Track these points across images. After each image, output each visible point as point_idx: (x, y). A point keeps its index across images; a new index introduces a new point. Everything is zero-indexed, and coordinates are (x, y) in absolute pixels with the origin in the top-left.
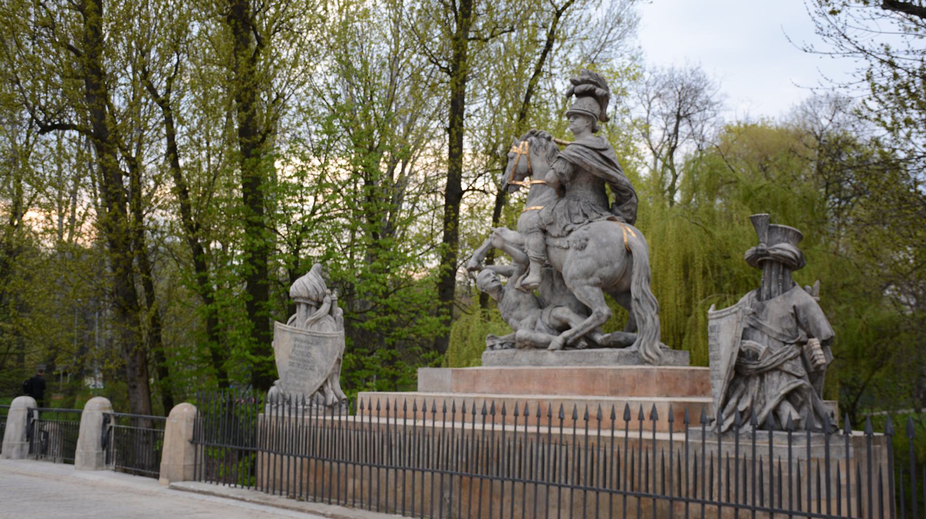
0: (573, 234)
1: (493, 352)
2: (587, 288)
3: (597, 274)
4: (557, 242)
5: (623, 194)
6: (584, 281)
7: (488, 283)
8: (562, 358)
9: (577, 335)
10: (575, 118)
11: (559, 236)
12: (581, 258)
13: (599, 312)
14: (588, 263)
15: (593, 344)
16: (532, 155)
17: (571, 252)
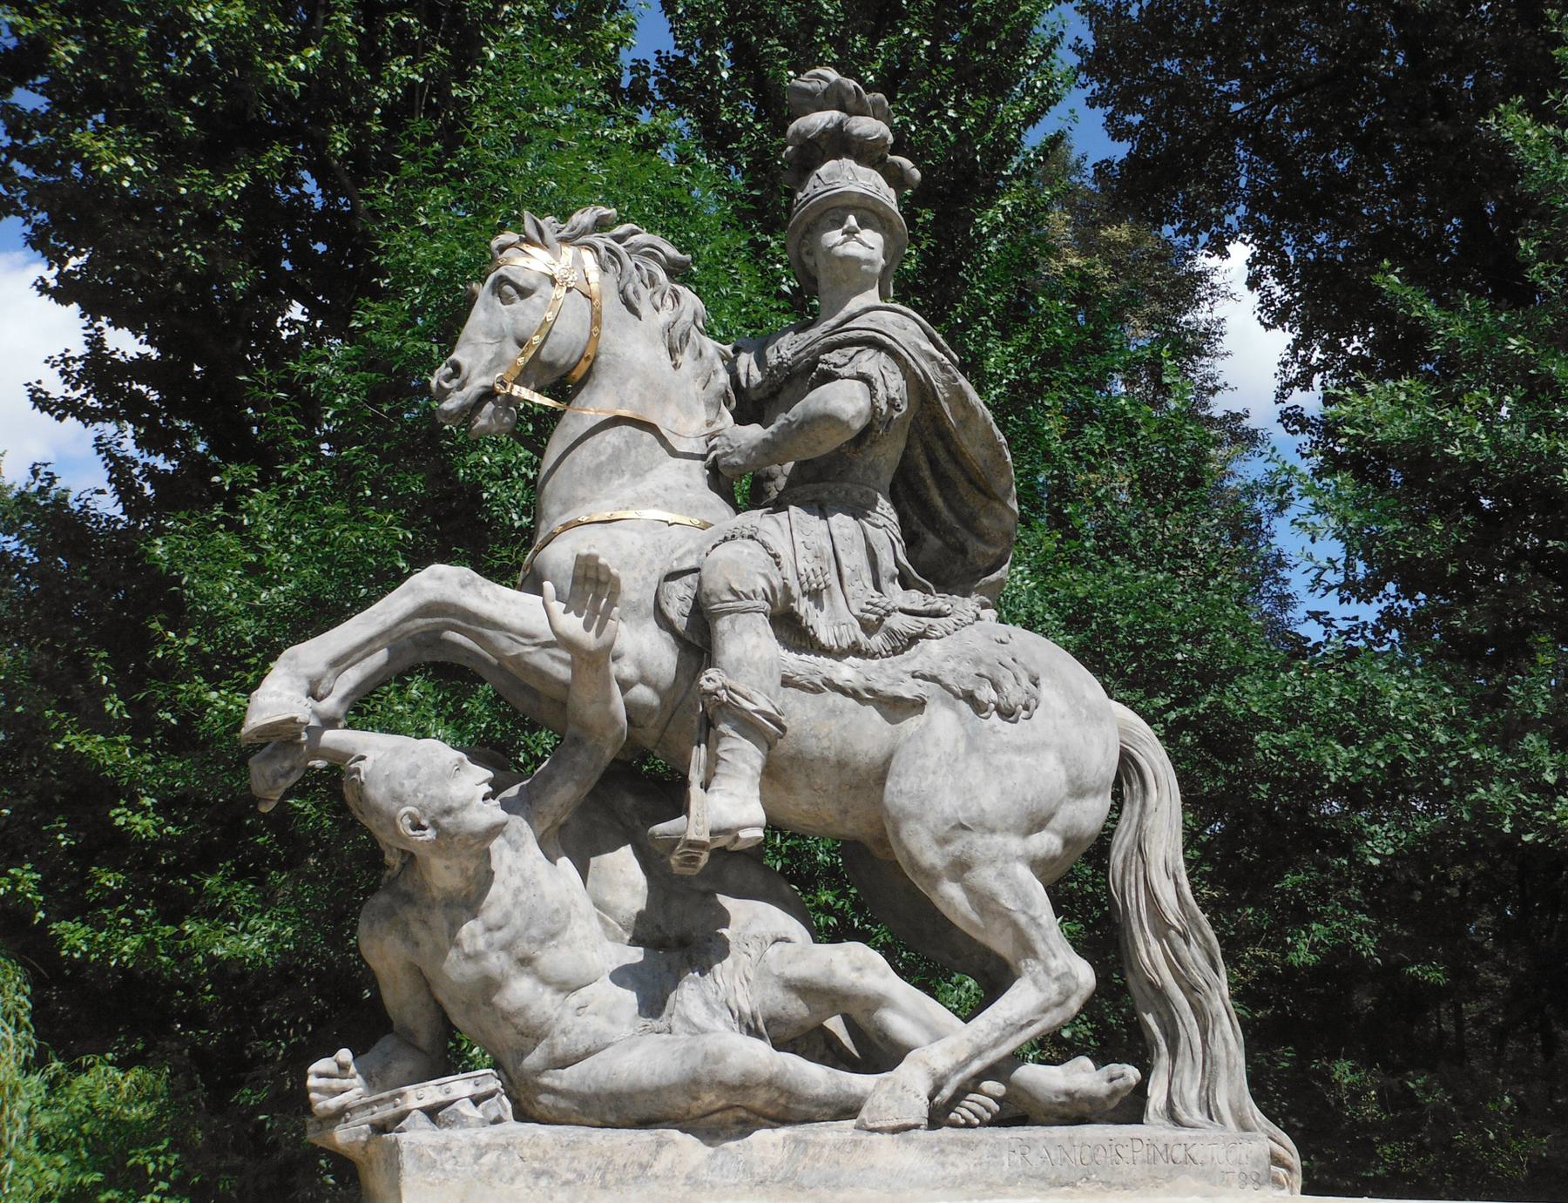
0: (932, 647)
1: (442, 1135)
2: (1024, 873)
3: (1058, 822)
4: (846, 671)
5: (975, 546)
6: (1015, 844)
7: (465, 806)
8: (961, 1164)
9: (976, 1066)
10: (863, 224)
11: (856, 650)
12: (1019, 750)
13: (1068, 974)
14: (1050, 773)
15: (1018, 1112)
16: (612, 306)
17: (943, 723)
